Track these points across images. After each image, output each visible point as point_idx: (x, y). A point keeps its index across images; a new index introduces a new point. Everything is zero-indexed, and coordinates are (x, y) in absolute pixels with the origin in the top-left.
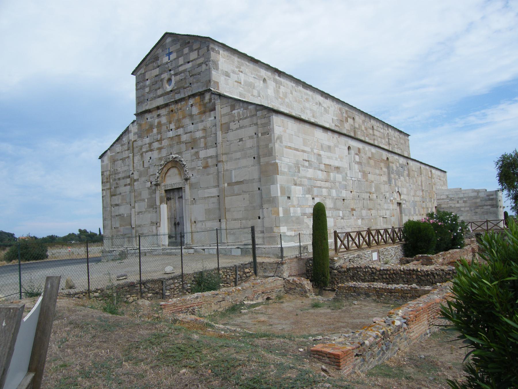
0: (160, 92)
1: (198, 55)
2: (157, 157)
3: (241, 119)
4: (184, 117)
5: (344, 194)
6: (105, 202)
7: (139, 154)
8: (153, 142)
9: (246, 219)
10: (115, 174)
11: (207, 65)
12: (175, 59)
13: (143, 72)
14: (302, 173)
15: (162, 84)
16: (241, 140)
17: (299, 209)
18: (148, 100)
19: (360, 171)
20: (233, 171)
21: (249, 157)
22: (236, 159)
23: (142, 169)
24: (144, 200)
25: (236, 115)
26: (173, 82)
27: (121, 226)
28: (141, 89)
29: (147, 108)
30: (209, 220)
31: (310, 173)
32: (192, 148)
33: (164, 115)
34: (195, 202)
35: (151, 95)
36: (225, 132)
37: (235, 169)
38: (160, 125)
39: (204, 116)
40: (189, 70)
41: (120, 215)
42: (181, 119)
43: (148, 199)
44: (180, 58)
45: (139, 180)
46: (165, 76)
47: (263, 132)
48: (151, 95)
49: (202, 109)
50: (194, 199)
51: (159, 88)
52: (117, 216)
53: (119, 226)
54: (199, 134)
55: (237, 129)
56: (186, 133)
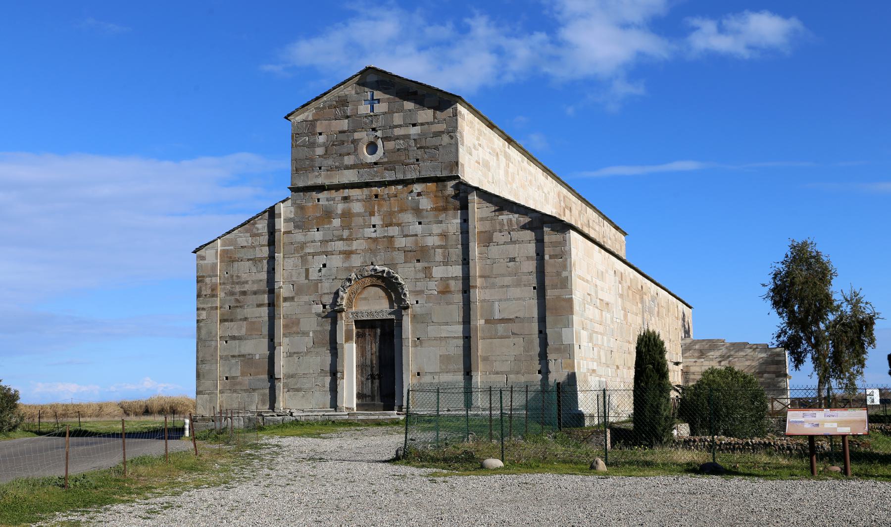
0: (349, 160)
1: (435, 118)
2: (340, 264)
3: (513, 230)
4: (402, 210)
6: (203, 332)
7: (296, 255)
8: (331, 241)
9: (518, 373)
10: (233, 283)
11: (452, 137)
12: (384, 113)
13: (310, 118)
15: (356, 150)
16: (513, 260)
17: (585, 361)
18: (320, 168)
20: (497, 304)
21: (525, 285)
22: (503, 287)
23: (302, 280)
24: (305, 334)
25: (505, 221)
26: (380, 151)
27: (243, 374)
28: (303, 146)
29: (320, 181)
30: (447, 372)
32: (418, 261)
33: (357, 200)
34: (421, 343)
35: (330, 162)
36: (484, 244)
37: (500, 300)
38: (347, 216)
39: (444, 215)
40: (415, 138)
41: (243, 356)
42: (395, 212)
43: (314, 332)
44: (396, 115)
45: (296, 300)
46: (364, 137)
47: (552, 254)
48: (330, 162)
49: (441, 204)
50: (418, 339)
51: (349, 154)
52: (233, 356)
53: (239, 374)
54: (431, 241)
55: (505, 243)
56: (406, 236)
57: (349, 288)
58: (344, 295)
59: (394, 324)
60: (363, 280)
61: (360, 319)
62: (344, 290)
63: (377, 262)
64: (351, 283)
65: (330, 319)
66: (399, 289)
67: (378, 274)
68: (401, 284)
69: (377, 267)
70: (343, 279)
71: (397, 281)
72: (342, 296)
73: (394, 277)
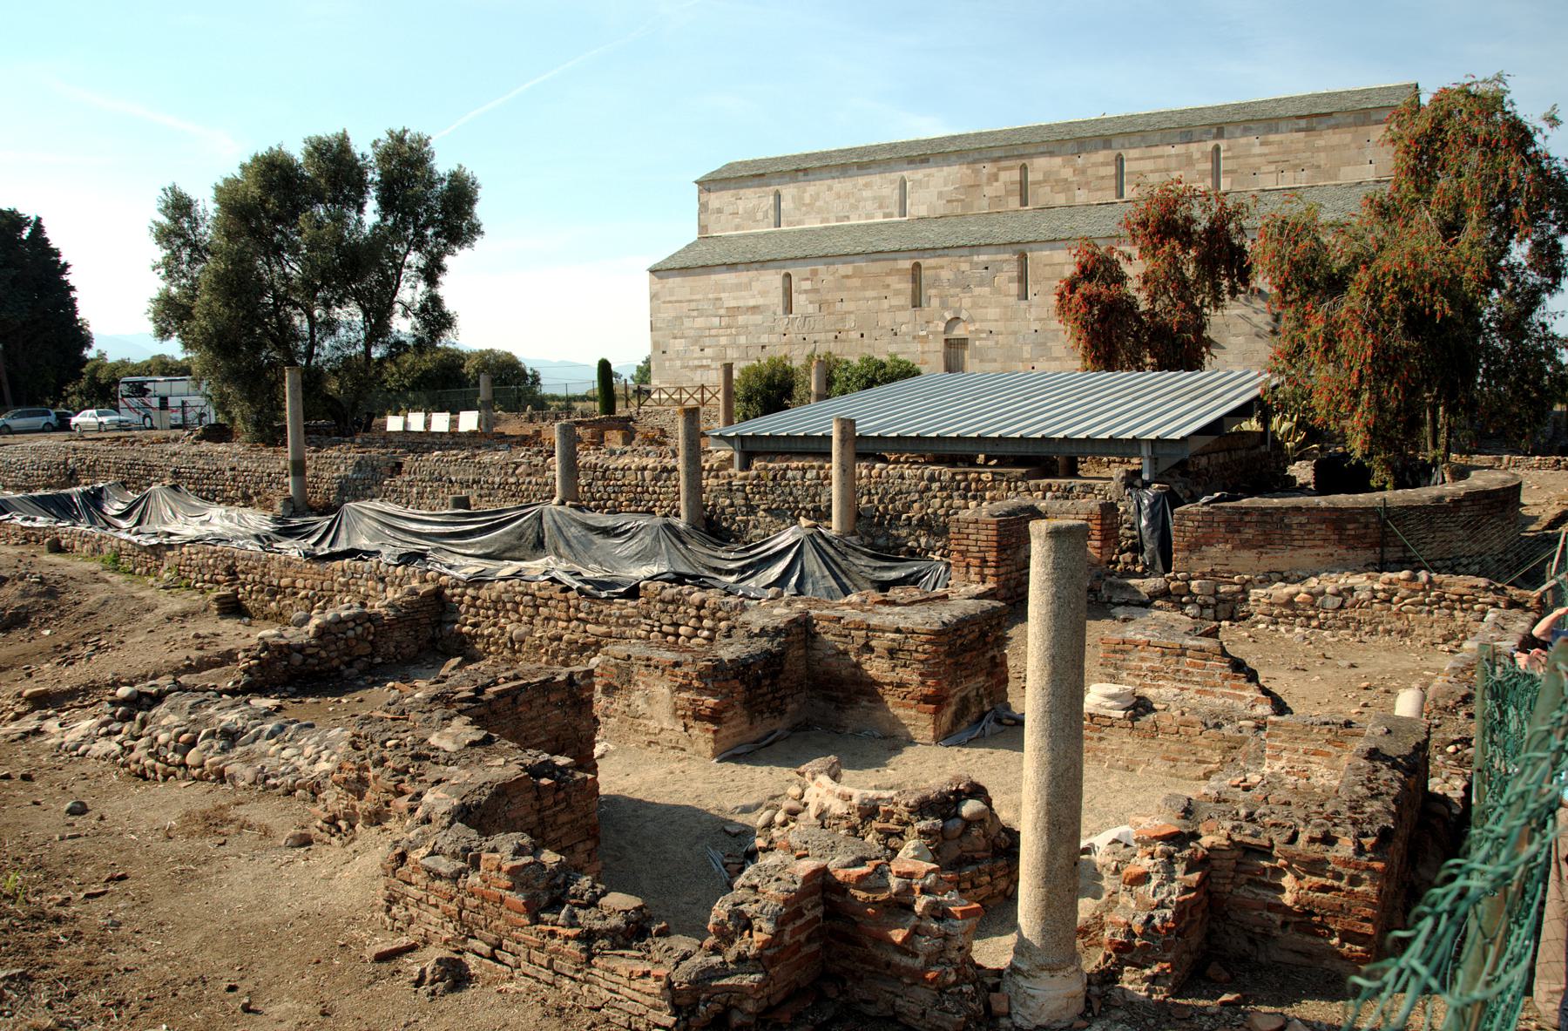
5: (764, 339)
14: (687, 323)
19: (811, 302)
31: (700, 322)
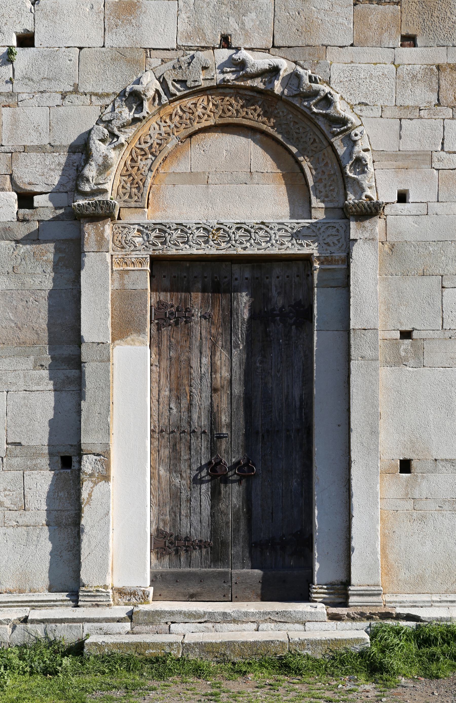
57: (131, 131)
58: (113, 154)
59: (312, 274)
60: (188, 102)
61: (173, 251)
62: (113, 135)
63: (247, 35)
64: (140, 107)
65: (51, 247)
66: (337, 142)
67: (249, 83)
68: (343, 121)
69: (244, 54)
70: (108, 95)
71: (331, 111)
72: (106, 157)
73: (317, 93)
